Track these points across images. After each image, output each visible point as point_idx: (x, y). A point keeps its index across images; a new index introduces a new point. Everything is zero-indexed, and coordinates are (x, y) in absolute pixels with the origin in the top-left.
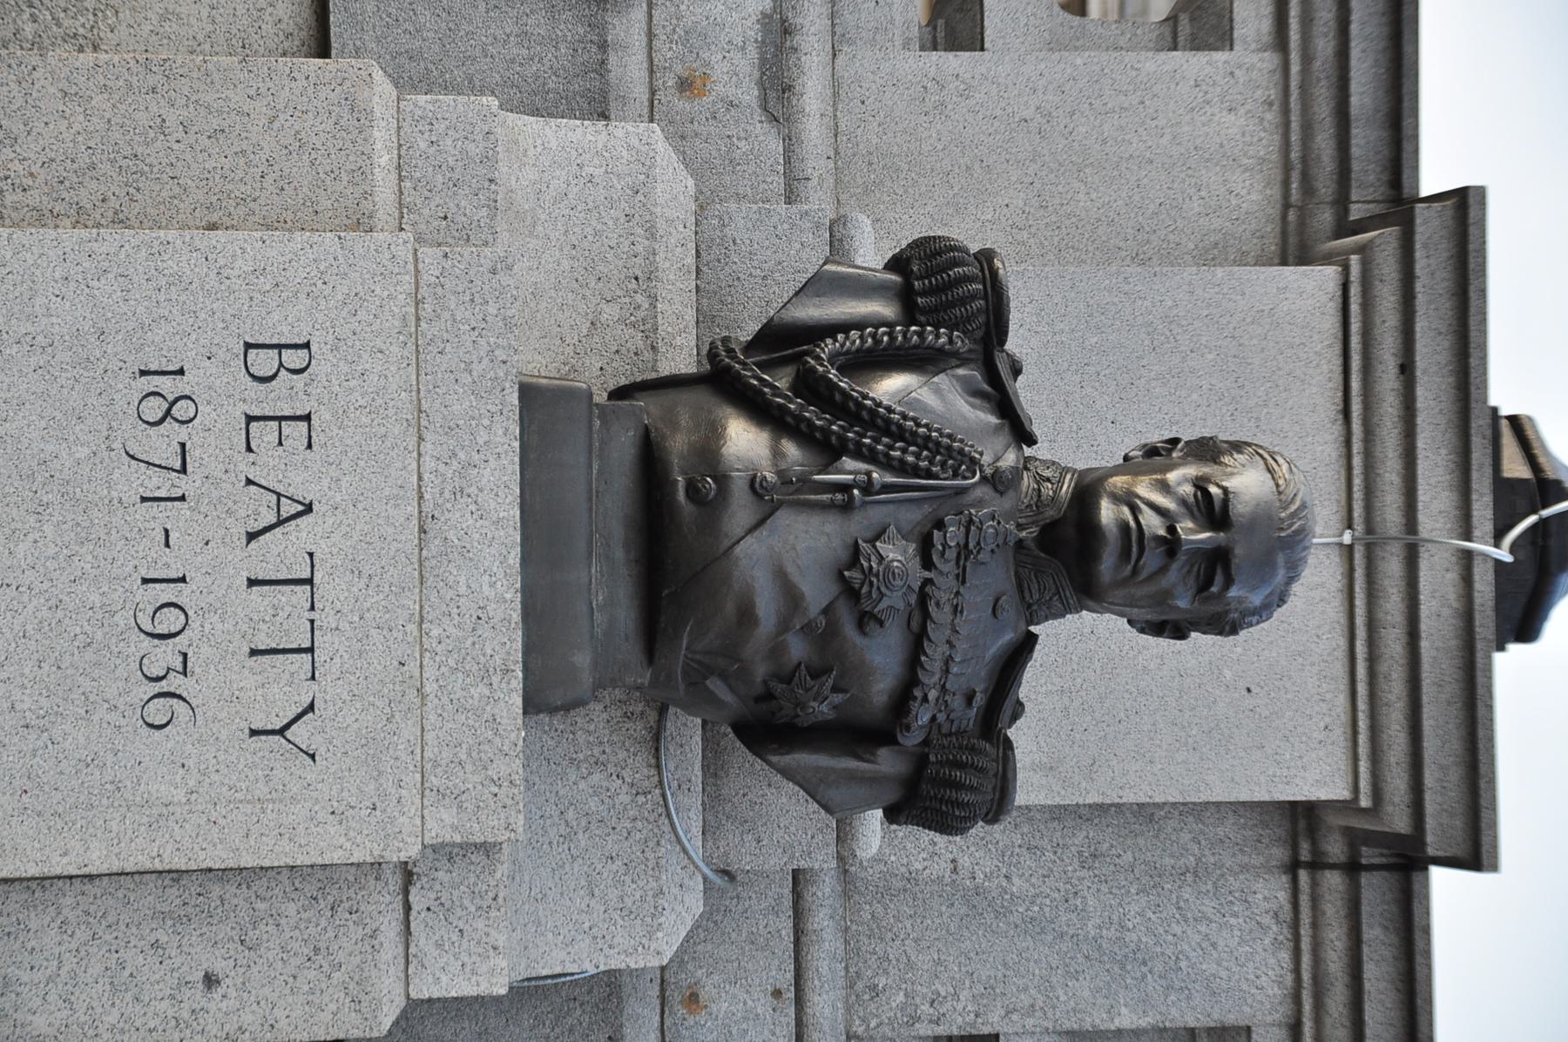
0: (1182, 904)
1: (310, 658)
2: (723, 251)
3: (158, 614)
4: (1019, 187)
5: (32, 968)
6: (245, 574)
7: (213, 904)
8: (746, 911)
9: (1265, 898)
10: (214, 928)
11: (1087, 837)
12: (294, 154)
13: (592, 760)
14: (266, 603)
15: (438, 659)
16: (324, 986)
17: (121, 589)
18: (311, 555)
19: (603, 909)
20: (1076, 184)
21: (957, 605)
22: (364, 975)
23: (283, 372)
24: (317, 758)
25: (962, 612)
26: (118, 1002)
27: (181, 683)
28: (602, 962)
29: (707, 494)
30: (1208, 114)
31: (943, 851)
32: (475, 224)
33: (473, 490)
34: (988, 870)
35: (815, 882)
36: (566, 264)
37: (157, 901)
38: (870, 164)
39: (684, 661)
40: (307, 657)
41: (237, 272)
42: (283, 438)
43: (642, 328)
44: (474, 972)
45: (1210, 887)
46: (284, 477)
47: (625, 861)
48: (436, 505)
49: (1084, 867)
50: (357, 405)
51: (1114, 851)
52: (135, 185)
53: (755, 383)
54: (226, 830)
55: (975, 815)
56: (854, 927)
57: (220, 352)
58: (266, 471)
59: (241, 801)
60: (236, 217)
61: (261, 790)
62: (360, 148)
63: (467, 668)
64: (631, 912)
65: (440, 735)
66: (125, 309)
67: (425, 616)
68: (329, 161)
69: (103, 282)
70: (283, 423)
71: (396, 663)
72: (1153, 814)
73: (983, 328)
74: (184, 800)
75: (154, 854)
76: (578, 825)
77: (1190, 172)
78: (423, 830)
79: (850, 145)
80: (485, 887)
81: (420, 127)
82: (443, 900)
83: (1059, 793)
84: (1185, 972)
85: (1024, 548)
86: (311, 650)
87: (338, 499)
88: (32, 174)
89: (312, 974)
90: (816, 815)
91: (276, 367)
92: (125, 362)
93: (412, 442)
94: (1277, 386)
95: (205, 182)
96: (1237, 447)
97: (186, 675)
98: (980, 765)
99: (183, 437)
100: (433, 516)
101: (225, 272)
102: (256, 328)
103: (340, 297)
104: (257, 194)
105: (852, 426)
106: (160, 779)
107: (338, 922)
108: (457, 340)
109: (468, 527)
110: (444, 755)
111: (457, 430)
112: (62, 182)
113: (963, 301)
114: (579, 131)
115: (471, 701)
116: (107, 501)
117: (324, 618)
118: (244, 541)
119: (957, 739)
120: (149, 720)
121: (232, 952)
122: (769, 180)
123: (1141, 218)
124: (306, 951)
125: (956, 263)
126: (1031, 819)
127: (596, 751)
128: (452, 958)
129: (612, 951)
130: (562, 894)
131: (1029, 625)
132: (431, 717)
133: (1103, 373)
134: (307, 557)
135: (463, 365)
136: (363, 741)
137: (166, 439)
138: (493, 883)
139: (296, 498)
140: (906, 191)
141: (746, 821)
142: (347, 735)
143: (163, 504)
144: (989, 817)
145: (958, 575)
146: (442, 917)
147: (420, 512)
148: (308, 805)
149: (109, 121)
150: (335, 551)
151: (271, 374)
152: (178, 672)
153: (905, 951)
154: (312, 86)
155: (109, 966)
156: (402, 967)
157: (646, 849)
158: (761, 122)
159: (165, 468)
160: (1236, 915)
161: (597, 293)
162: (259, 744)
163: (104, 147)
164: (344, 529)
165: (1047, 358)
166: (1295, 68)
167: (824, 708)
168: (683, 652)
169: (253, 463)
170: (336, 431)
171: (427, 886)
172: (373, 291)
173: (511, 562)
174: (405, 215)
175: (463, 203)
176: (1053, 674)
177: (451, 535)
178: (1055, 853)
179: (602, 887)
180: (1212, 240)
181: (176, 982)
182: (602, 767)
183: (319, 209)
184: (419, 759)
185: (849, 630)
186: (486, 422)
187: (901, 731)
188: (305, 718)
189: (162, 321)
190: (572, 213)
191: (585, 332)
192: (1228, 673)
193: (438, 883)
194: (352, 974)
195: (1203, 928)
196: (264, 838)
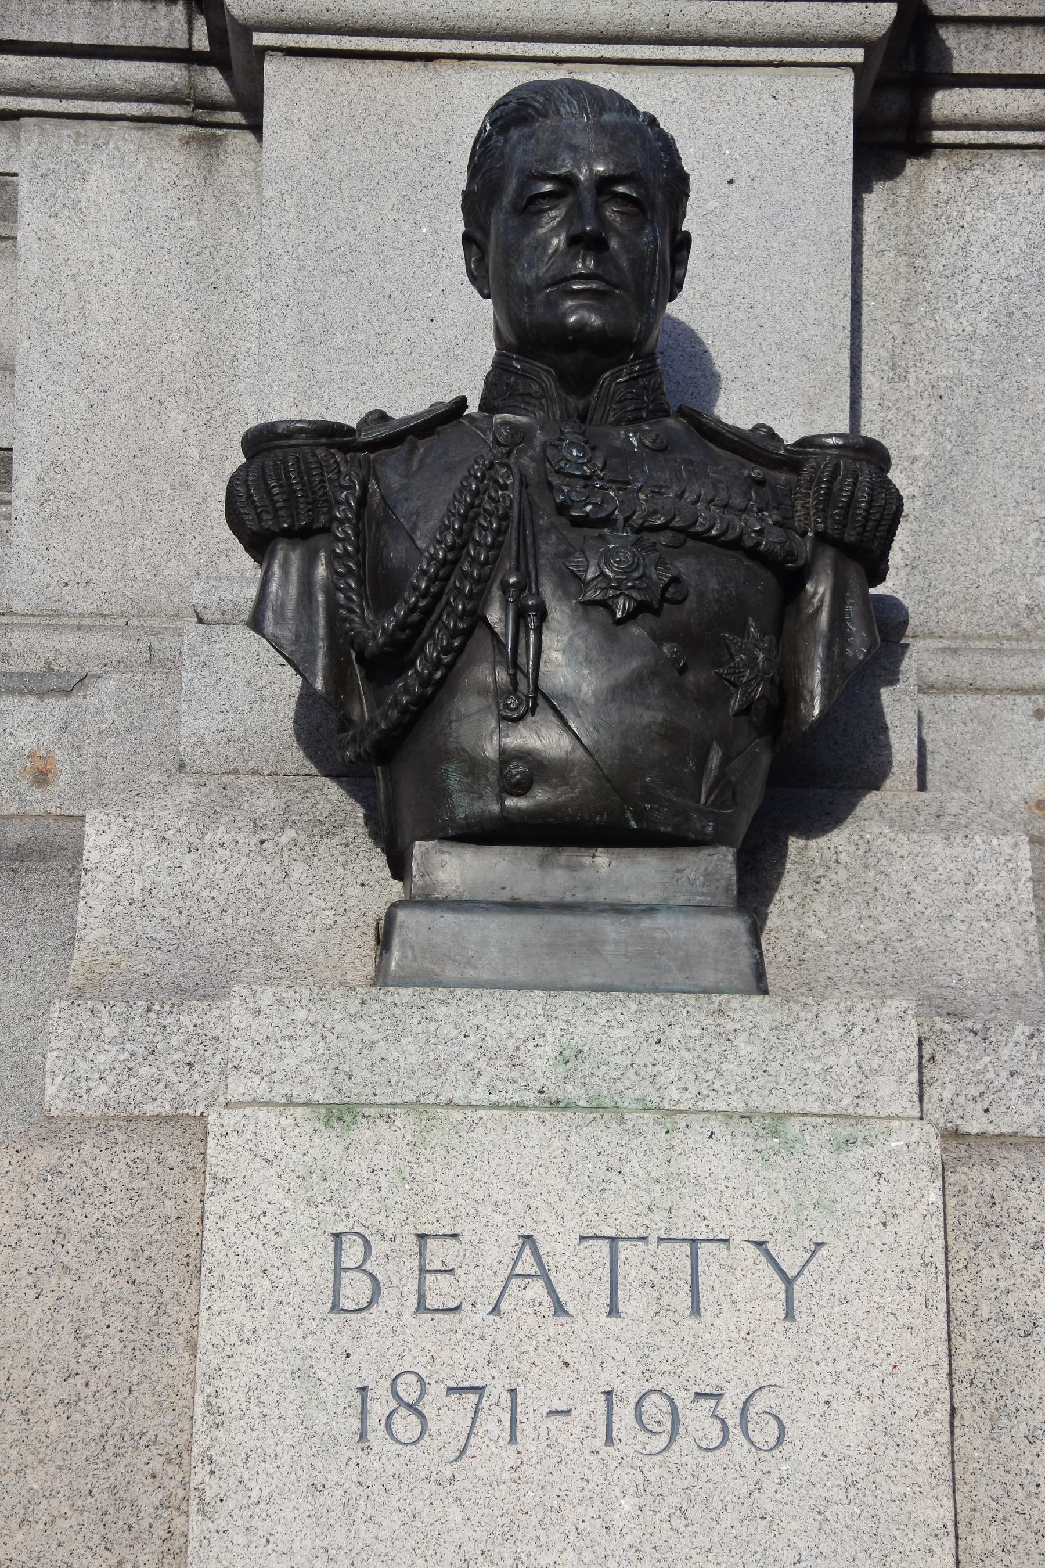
0: (947, 272)
1: (703, 1244)
2: (231, 743)
3: (649, 1427)
4: (164, 417)
6: (604, 1319)
12: (108, 1244)
13: (800, 911)
14: (636, 1295)
17: (619, 1471)
18: (582, 1238)
20: (163, 354)
23: (368, 1266)
24: (819, 1241)
27: (730, 1401)
30: (87, 204)
32: (199, 1031)
33: (511, 1044)
40: (703, 1249)
41: (247, 1320)
45: (931, 242)
47: (912, 878)
48: (527, 1087)
49: (905, 378)
51: (889, 345)
52: (137, 1438)
54: (904, 1353)
58: (483, 1290)
59: (870, 1334)
60: (181, 1315)
62: (105, 1164)
63: (716, 1057)
65: (792, 1093)
66: (285, 1459)
67: (654, 1105)
71: (711, 1142)
74: (868, 1402)
75: (931, 1442)
77: (152, 228)
81: (83, 1092)
84: (1022, 271)
92: (350, 1459)
94: (396, 135)
95: (137, 1352)
100: (540, 1092)
101: (247, 1334)
102: (314, 1297)
103: (281, 1195)
104: (154, 1289)
106: (843, 1432)
107: (1005, 1220)
108: (336, 1058)
111: (441, 1061)
112: (130, 1527)
114: (91, 903)
115: (755, 1055)
116: (514, 1486)
120: (772, 1442)
123: (202, 285)
129: (1014, 897)
134: (585, 1244)
135: (366, 1052)
136: (801, 1184)
137: (442, 1411)
140: (166, 541)
143: (519, 1417)
146: (995, 1096)
147: (535, 1107)
149: (59, 1468)
150: (579, 1211)
151: (369, 1281)
152: (717, 1405)
154: (28, 1221)
158: (85, 697)
159: (476, 1412)
163: (90, 1474)
164: (553, 1199)
170: (437, 1205)
171: (960, 1112)
174: (186, 1111)
182: (808, 900)
183: (174, 1214)
184: (822, 1119)
186: (432, 1026)
188: (773, 1253)
192: (713, 204)
195: (975, 250)
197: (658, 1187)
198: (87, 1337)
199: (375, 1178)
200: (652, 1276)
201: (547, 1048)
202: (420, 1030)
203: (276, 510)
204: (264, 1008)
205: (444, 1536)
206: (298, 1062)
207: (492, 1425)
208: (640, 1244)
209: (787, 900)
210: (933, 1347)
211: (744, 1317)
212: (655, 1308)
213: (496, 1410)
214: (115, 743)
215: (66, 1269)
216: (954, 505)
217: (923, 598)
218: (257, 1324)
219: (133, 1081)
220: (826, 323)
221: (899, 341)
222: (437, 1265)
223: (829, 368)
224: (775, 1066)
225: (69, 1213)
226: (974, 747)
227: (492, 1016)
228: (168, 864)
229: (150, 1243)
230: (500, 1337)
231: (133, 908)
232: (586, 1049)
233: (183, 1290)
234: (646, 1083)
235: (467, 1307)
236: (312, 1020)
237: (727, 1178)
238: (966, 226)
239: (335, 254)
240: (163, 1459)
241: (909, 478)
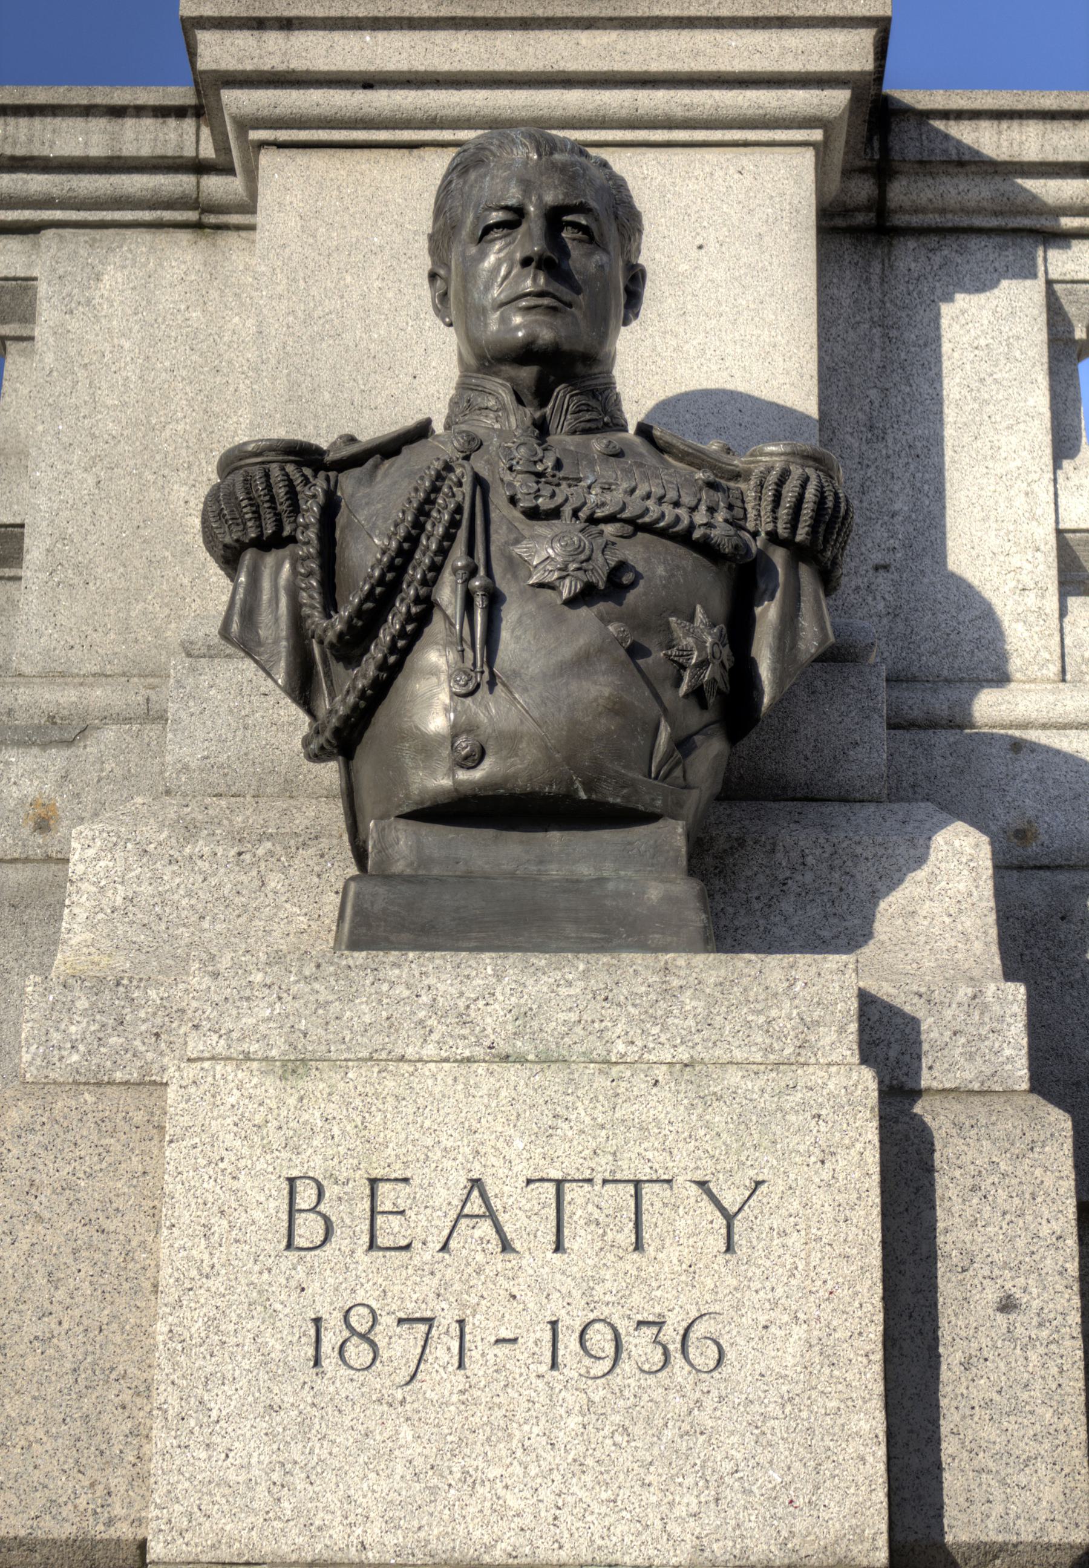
0: (921, 342)
4: (167, 490)
5: (989, 1501)
6: (550, 1255)
12: (79, 1195)
15: (651, 1045)
18: (529, 1182)
19: (928, 902)
20: (167, 433)
23: (322, 1208)
24: (760, 1178)
26: (1028, 1408)
32: (165, 1003)
33: (462, 1003)
40: (646, 1189)
41: (206, 1256)
43: (293, 849)
46: (440, 1209)
48: (478, 1043)
51: (867, 408)
54: (840, 1280)
57: (297, 1277)
58: (434, 1230)
59: (808, 1264)
60: (148, 1262)
66: (243, 1382)
69: (212, 1405)
70: (379, 1209)
71: (655, 1090)
74: (805, 1327)
75: (865, 1360)
77: (160, 320)
81: (55, 1060)
86: (637, 1184)
87: (467, 1150)
88: (92, 1485)
89: (1002, 1194)
93: (406, 1068)
94: (381, 213)
99: (391, 1320)
102: (270, 1236)
103: (238, 1143)
104: (122, 1238)
110: (759, 1040)
112: (102, 1453)
114: (76, 910)
115: (699, 1010)
116: (463, 1407)
117: (603, 1166)
118: (511, 1256)
120: (712, 1364)
122: (147, 740)
124: (975, 1201)
125: (231, 495)
127: (757, 906)
129: (975, 893)
134: (532, 1186)
135: (321, 1011)
136: (742, 1127)
140: (167, 605)
143: (467, 1345)
147: (484, 1061)
149: (35, 1398)
150: (525, 1155)
153: (971, 621)
156: (995, 1098)
158: (85, 747)
166: (58, 215)
169: (424, 1244)
170: (389, 1151)
171: (905, 1069)
183: (140, 1169)
186: (385, 987)
188: (714, 1191)
190: (165, 919)
197: (603, 1133)
198: (59, 1280)
199: (327, 1127)
200: (596, 1214)
201: (497, 1006)
205: (397, 1453)
207: (441, 1352)
213: (445, 1338)
215: (39, 1218)
219: (103, 1050)
221: (877, 404)
222: (388, 1206)
224: (719, 1019)
225: (41, 1167)
230: (449, 1272)
232: (534, 1007)
235: (417, 1245)
239: (321, 322)
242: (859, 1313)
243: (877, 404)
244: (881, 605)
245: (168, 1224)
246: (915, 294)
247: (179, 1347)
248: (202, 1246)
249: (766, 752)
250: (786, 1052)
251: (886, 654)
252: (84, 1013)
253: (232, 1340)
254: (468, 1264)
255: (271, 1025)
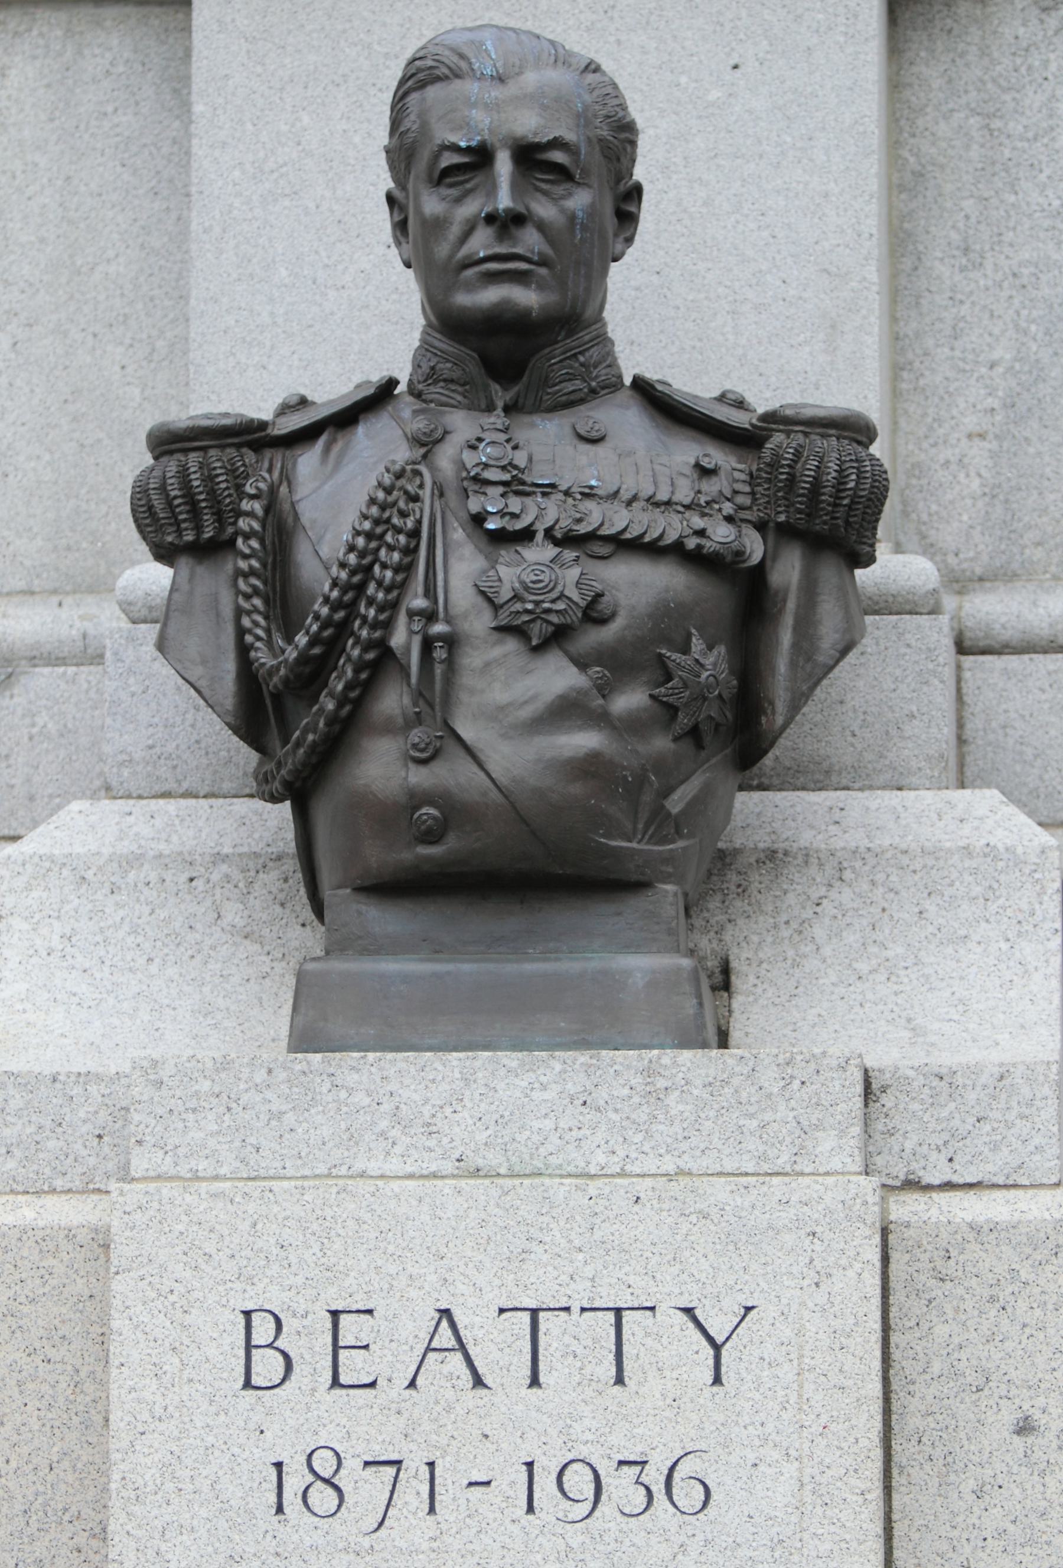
0: (1030, 135)
1: (628, 1312)
2: (162, 761)
3: (571, 1495)
4: (98, 352)
6: (525, 1392)
7: (932, 1425)
8: (1023, 717)
9: (1024, 25)
10: (961, 1424)
11: (942, 260)
12: (21, 1323)
13: (796, 936)
14: (559, 1366)
16: (1037, 1290)
17: (540, 1539)
18: (502, 1311)
19: (983, 924)
21: (582, 494)
22: (1025, 1240)
23: (278, 1344)
24: (750, 1304)
25: (591, 487)
26: (1045, 1538)
27: (654, 1468)
28: (1051, 925)
29: (434, 818)
31: (957, 451)
32: (107, 1101)
33: (427, 1111)
34: (982, 392)
35: (987, 625)
36: (172, 971)
37: (925, 1492)
38: (69, 548)
39: (648, 843)
40: (627, 1316)
41: (158, 1398)
42: (359, 1344)
43: (252, 873)
44: (1030, 1103)
45: (1007, 97)
46: (406, 1343)
47: (925, 895)
48: (444, 1157)
49: (981, 264)
50: (319, 1254)
51: (961, 225)
53: (302, 751)
54: (835, 1414)
55: (857, 461)
56: (1053, 569)
58: (398, 1366)
59: (800, 1396)
60: (98, 1394)
61: (788, 1373)
62: (13, 1241)
63: (646, 1118)
64: (990, 887)
65: (727, 1152)
67: (580, 1170)
68: (29, 1281)
69: (169, 1556)
70: (341, 1344)
71: (636, 1208)
72: (913, 173)
73: (244, 450)
74: (796, 1464)
75: (860, 1499)
76: (877, 957)
78: (843, 1173)
79: (45, 575)
80: (926, 1090)
82: (940, 1142)
83: (865, 318)
85: (517, 401)
86: (618, 1312)
87: (433, 1278)
90: (882, 642)
91: (272, 1352)
93: (364, 1187)
94: (344, 31)
96: (395, 124)
97: (646, 1462)
98: (790, 456)
99: (358, 1463)
101: (158, 1411)
102: (225, 1375)
103: (188, 1274)
104: (69, 1368)
105: (352, 633)
106: (770, 1493)
107: (960, 1273)
108: (242, 1130)
109: (472, 1117)
110: (752, 1147)
111: (352, 1130)
113: (209, 479)
115: (686, 1114)
116: (433, 1555)
119: (759, 485)
121: (991, 1402)
122: (85, 686)
124: (993, 1313)
125: (163, 488)
126: (917, 335)
128: (1012, 1131)
129: (1038, 912)
130: (962, 978)
131: (623, 385)
132: (704, 1164)
133: (326, 261)
135: (274, 1123)
136: (731, 1247)
137: (359, 1485)
138: (921, 1080)
139: (432, 1329)
141: (887, 733)
142: (723, 1267)
143: (437, 1489)
144: (864, 439)
145: (544, 494)
146: (961, 1144)
147: (454, 1176)
148: (807, 1315)
150: (497, 1282)
155: (1001, 1549)
156: (1020, 1193)
157: (911, 868)
158: (12, 697)
159: (394, 1486)
160: (1046, 63)
161: (208, 931)
162: (731, 1374)
165: (305, 334)
167: (709, 661)
168: (634, 845)
171: (922, 1163)
172: (182, 1233)
173: (514, 1064)
174: (97, 1186)
175: (82, 1114)
176: (713, 325)
177: (482, 1137)
178: (961, 302)
179: (956, 925)
180: (168, 97)
181: (1024, 1468)
182: (806, 925)
183: (87, 1293)
184: (755, 1179)
185: (607, 634)
186: (343, 1094)
187: (744, 561)
189: (218, 1487)
190: (108, 963)
191: (257, 947)
192: (714, 95)
193: (918, 1149)
194: (1023, 1256)
196: (845, 1368)
197: (581, 1256)
199: (283, 1254)
200: (575, 1346)
201: (466, 1114)
202: (330, 1098)
203: (178, 523)
204: (165, 1079)
206: (202, 1135)
207: (411, 1497)
208: (562, 1314)
209: (783, 926)
210: (864, 1407)
211: (669, 1385)
212: (577, 1378)
213: (414, 1483)
214: (47, 751)
216: (1041, 419)
217: (1006, 533)
218: (168, 1401)
219: (41, 1155)
220: (849, 231)
221: (973, 220)
223: (853, 284)
226: (1053, 719)
227: (406, 1082)
228: (90, 906)
229: (63, 1322)
231: (51, 958)
233: (99, 1369)
234: (570, 1147)
236: (217, 1091)
237: (654, 1244)
238: (1050, 77)
240: (86, 1534)
241: (987, 387)
242: (855, 1449)
243: (973, 220)
244: (976, 483)
245: (117, 1363)
246: (1023, 70)
247: (133, 1495)
248: (154, 1387)
249: (807, 727)
250: (780, 1161)
251: (981, 547)
252: (18, 1115)
253: (188, 1487)
254: (437, 1402)
255: (221, 1139)
